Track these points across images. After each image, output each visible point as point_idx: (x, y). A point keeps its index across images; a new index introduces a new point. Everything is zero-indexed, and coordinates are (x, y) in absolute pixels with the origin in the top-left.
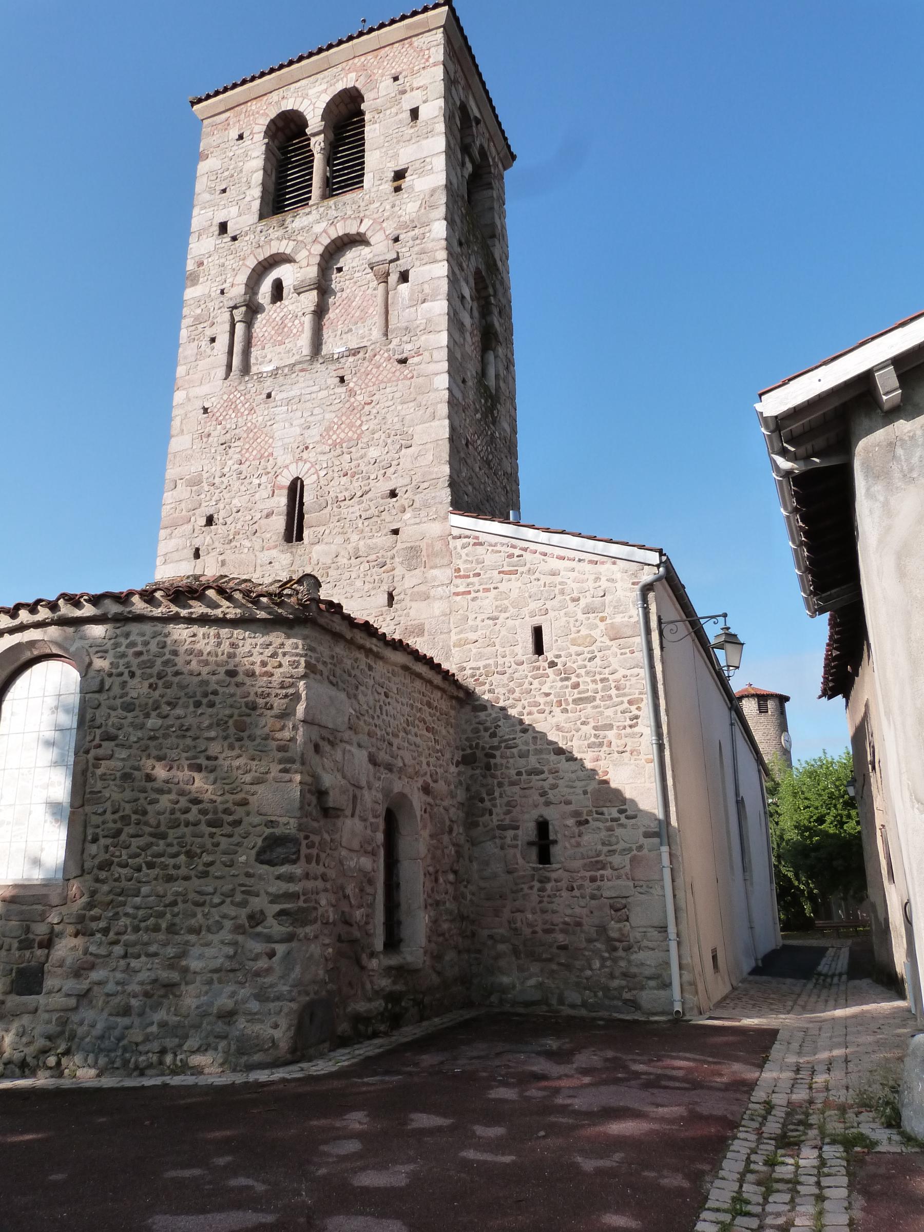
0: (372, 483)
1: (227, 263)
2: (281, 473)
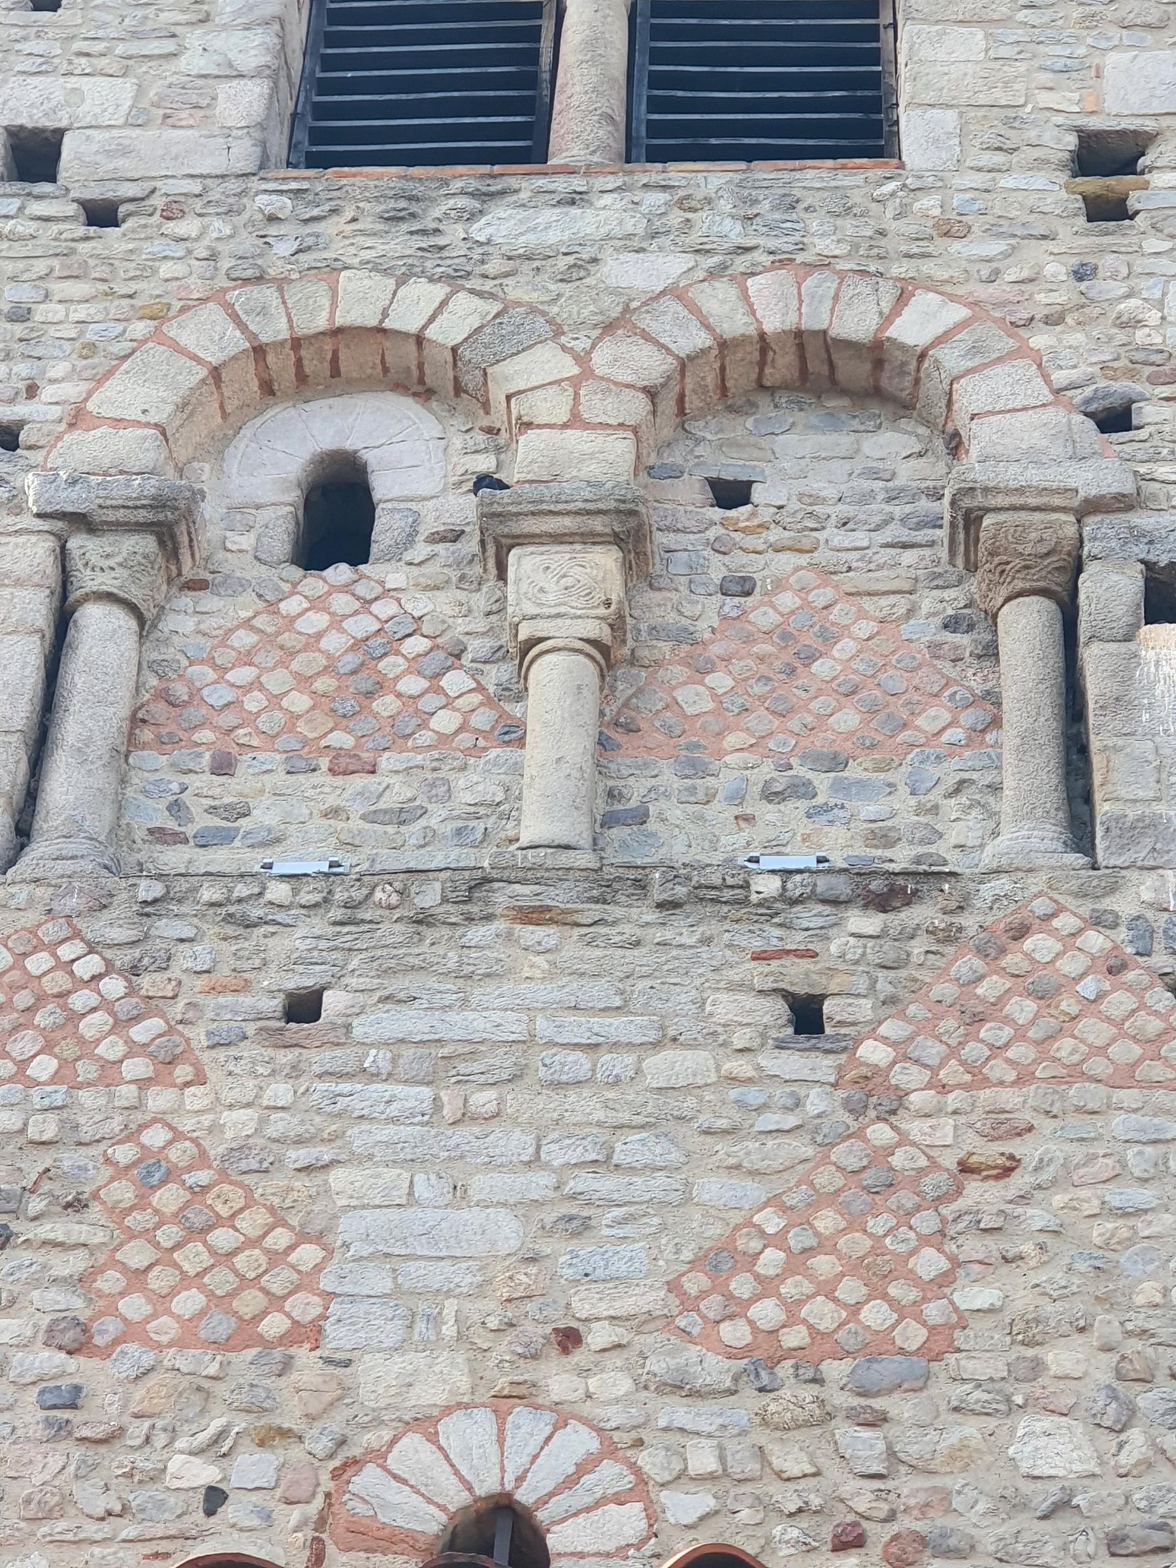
2: (379, 1456)
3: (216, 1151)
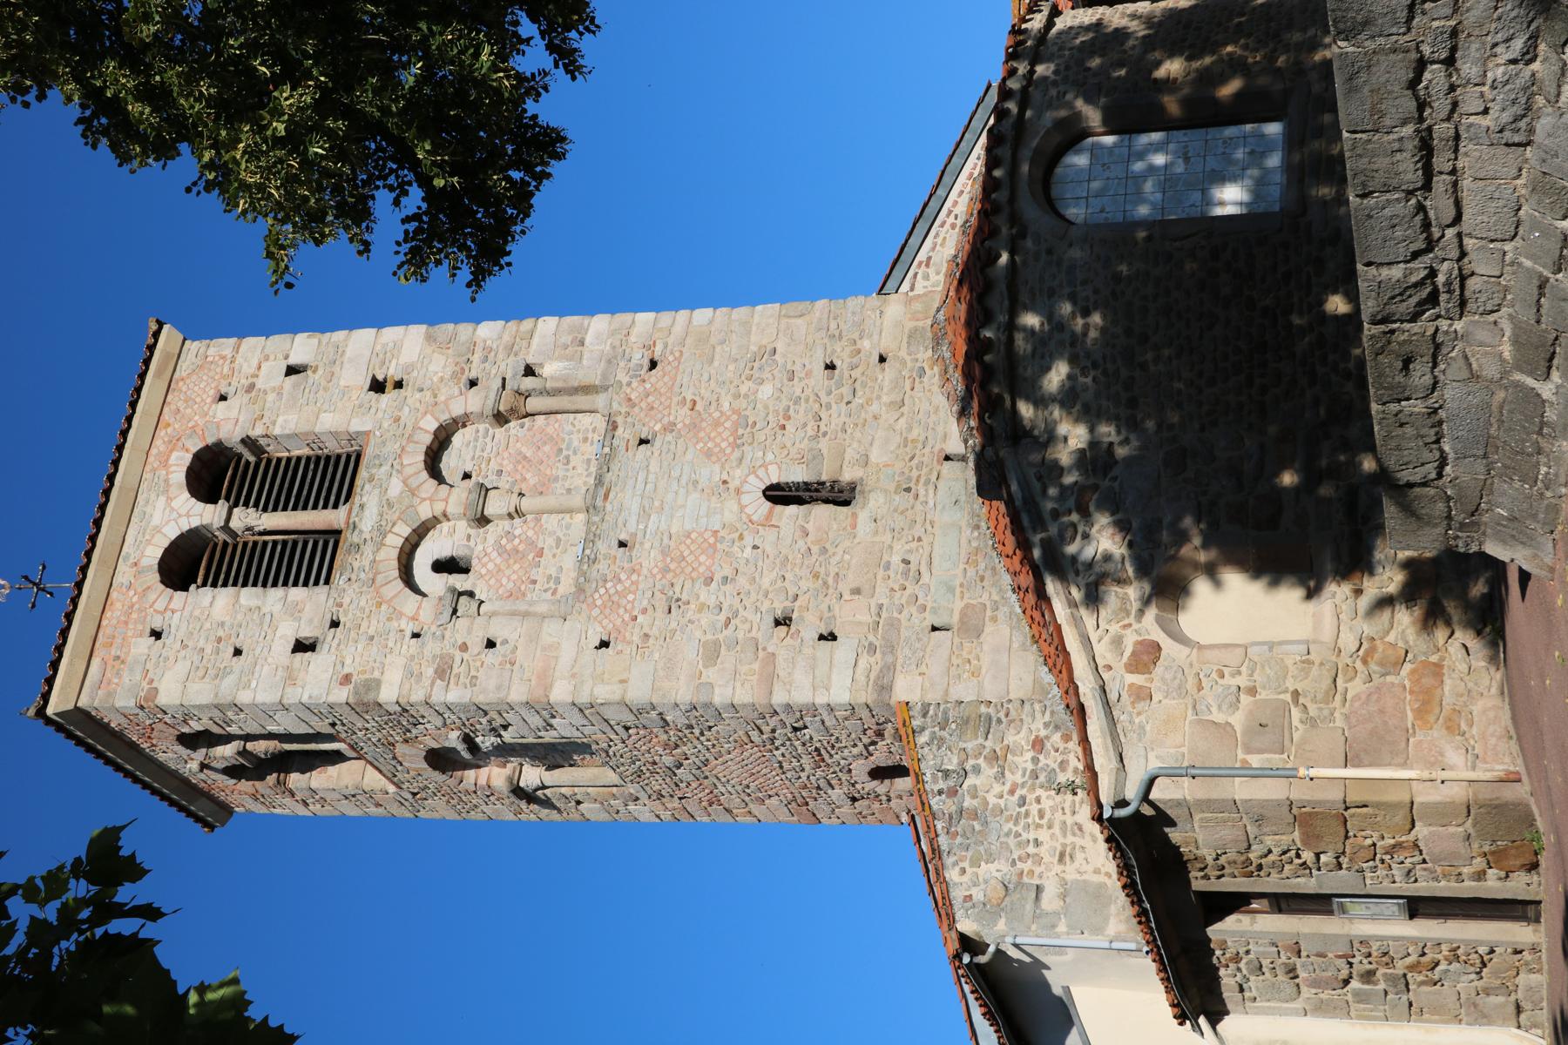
0: (808, 392)
1: (371, 632)
3: (660, 558)
